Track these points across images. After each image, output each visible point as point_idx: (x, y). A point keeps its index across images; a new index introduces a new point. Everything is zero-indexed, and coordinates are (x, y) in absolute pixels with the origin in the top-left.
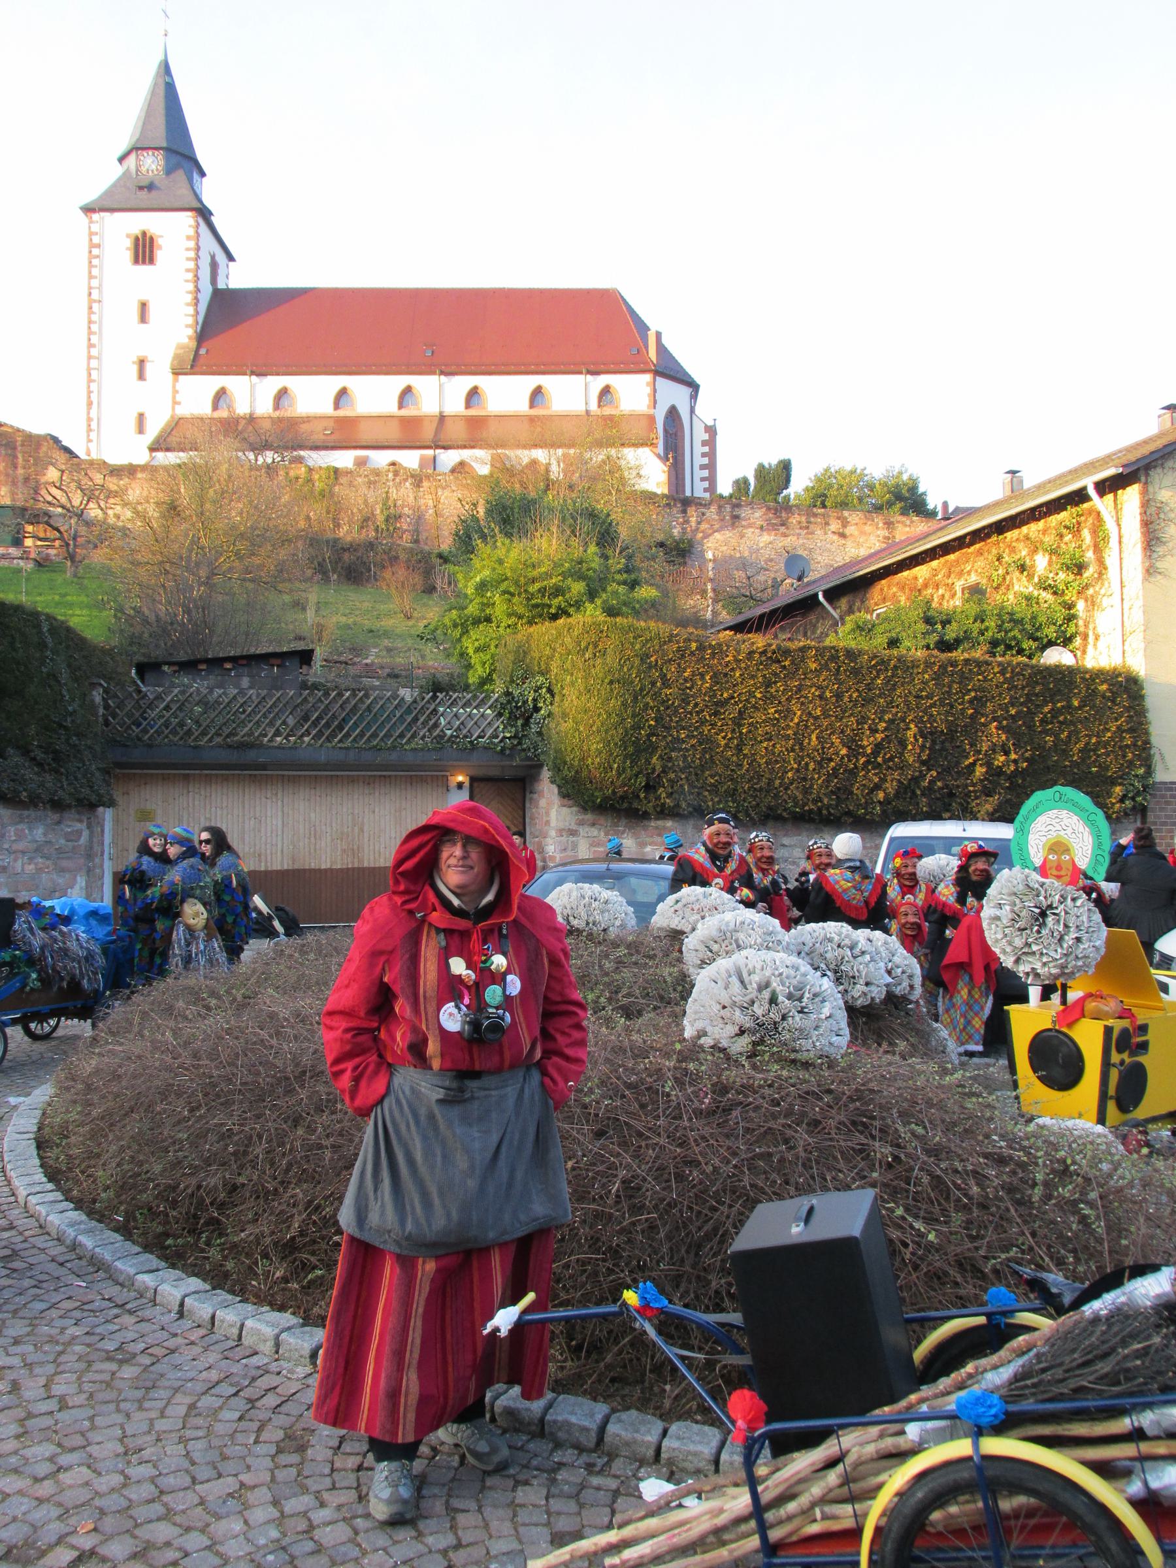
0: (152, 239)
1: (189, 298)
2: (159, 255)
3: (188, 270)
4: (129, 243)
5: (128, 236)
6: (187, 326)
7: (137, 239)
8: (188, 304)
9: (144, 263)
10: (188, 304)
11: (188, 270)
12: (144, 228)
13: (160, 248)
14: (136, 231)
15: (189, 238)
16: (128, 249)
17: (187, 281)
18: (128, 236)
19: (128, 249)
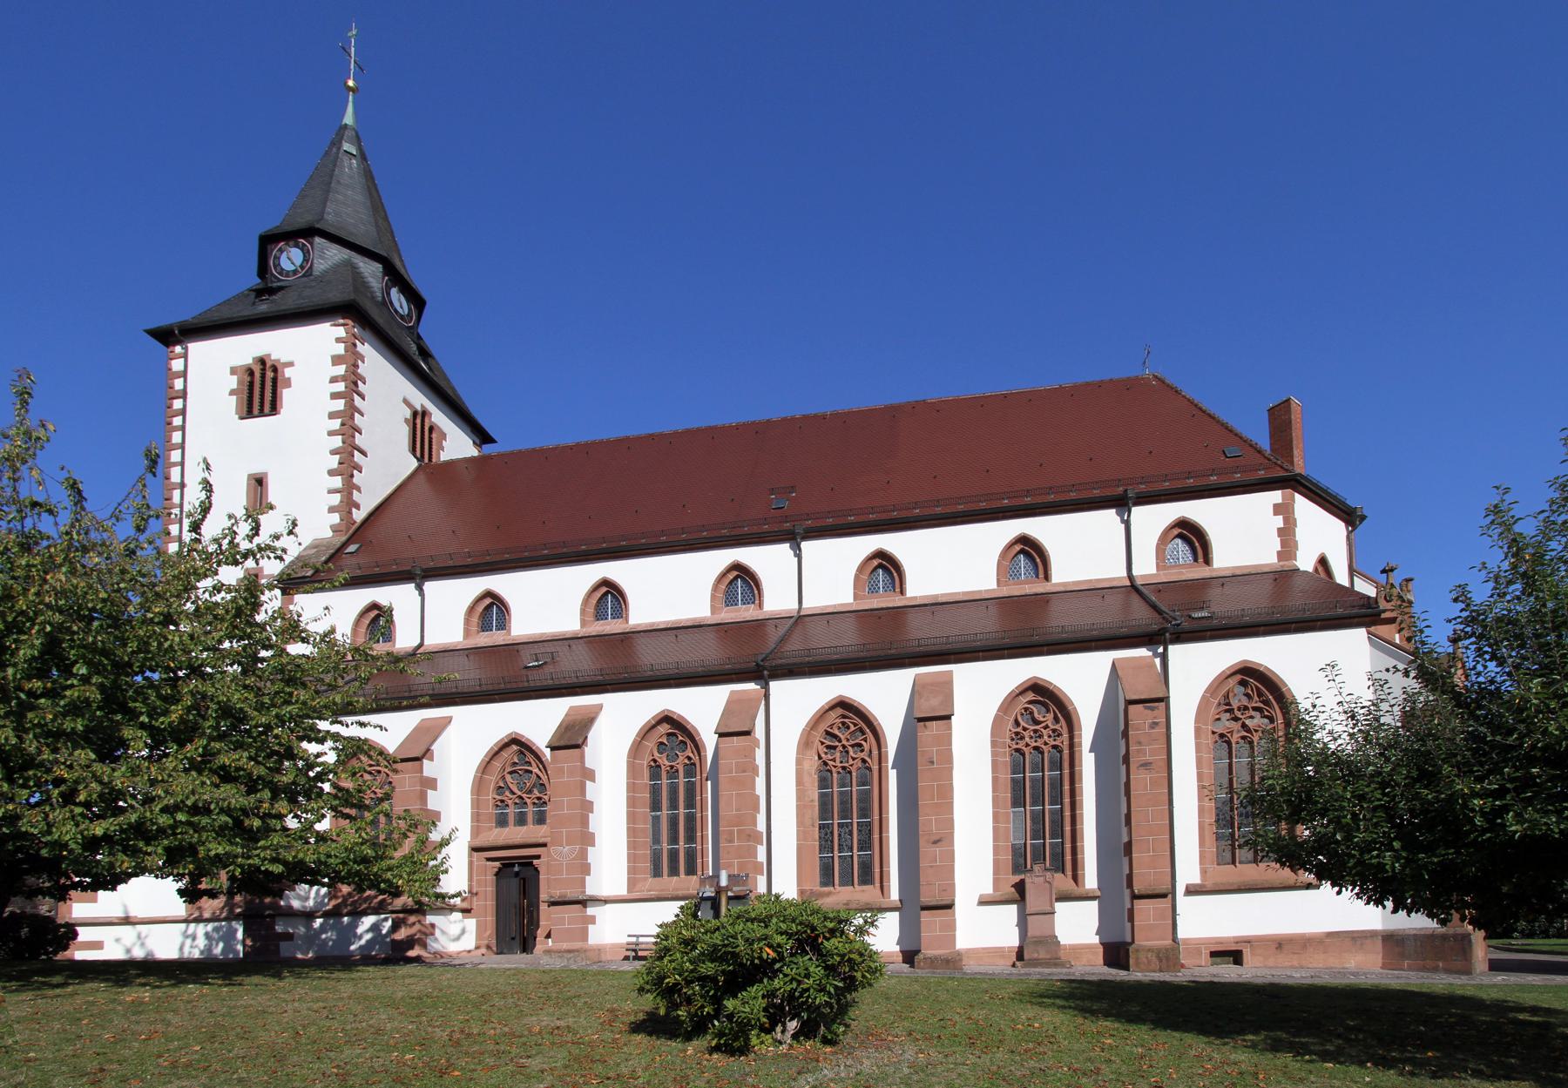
0: (275, 369)
1: (334, 461)
2: (286, 395)
3: (332, 416)
4: (233, 382)
5: (233, 371)
6: (332, 510)
7: (251, 373)
8: (332, 473)
9: (262, 414)
10: (332, 473)
11: (332, 416)
12: (260, 354)
13: (288, 383)
14: (247, 359)
15: (336, 360)
16: (232, 393)
17: (331, 433)
18: (233, 371)
19: (232, 393)
